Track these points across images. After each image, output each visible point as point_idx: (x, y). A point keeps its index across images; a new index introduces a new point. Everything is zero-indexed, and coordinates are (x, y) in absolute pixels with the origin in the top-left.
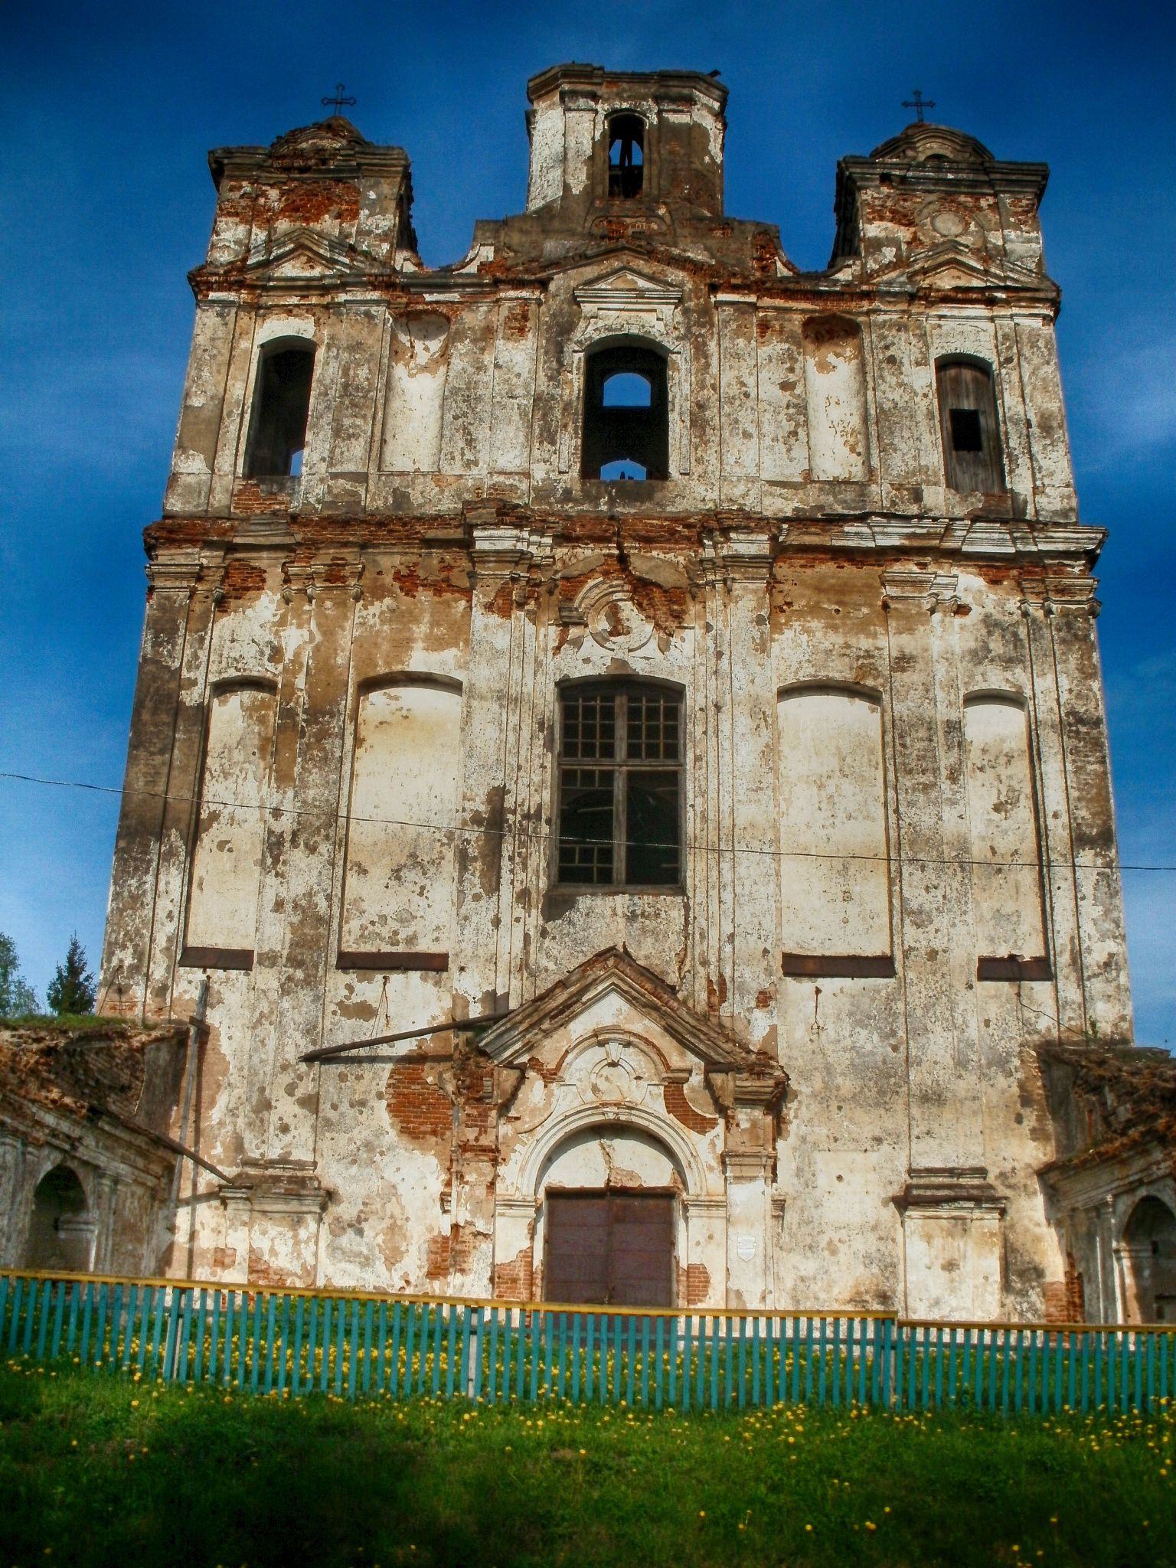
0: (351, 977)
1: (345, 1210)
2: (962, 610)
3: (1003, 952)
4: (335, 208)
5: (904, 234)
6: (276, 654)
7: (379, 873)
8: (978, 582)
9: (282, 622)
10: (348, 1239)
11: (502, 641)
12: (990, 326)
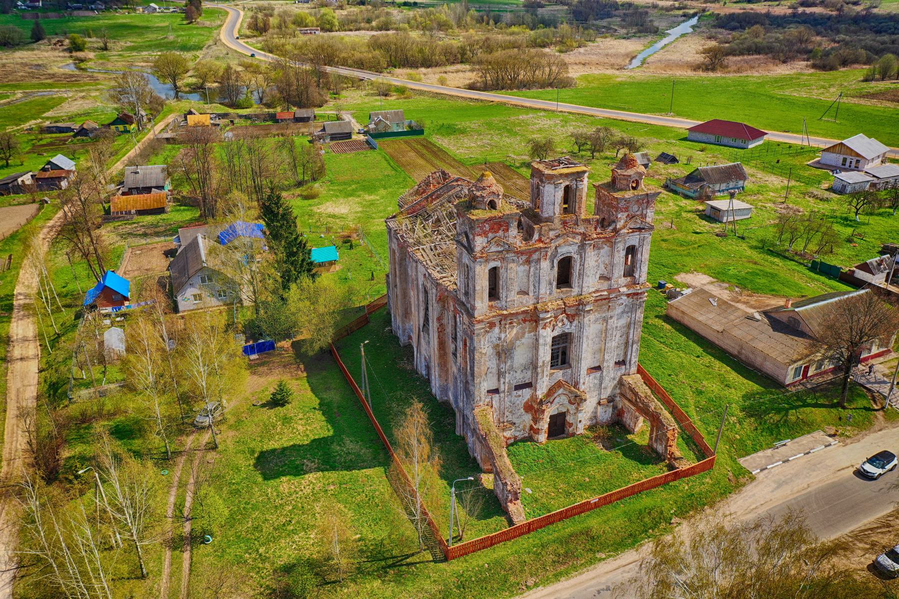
1: (517, 425)
3: (617, 361)
4: (502, 228)
5: (626, 214)
6: (500, 339)
7: (519, 372)
9: (501, 332)
10: (518, 429)
11: (545, 334)
12: (638, 236)
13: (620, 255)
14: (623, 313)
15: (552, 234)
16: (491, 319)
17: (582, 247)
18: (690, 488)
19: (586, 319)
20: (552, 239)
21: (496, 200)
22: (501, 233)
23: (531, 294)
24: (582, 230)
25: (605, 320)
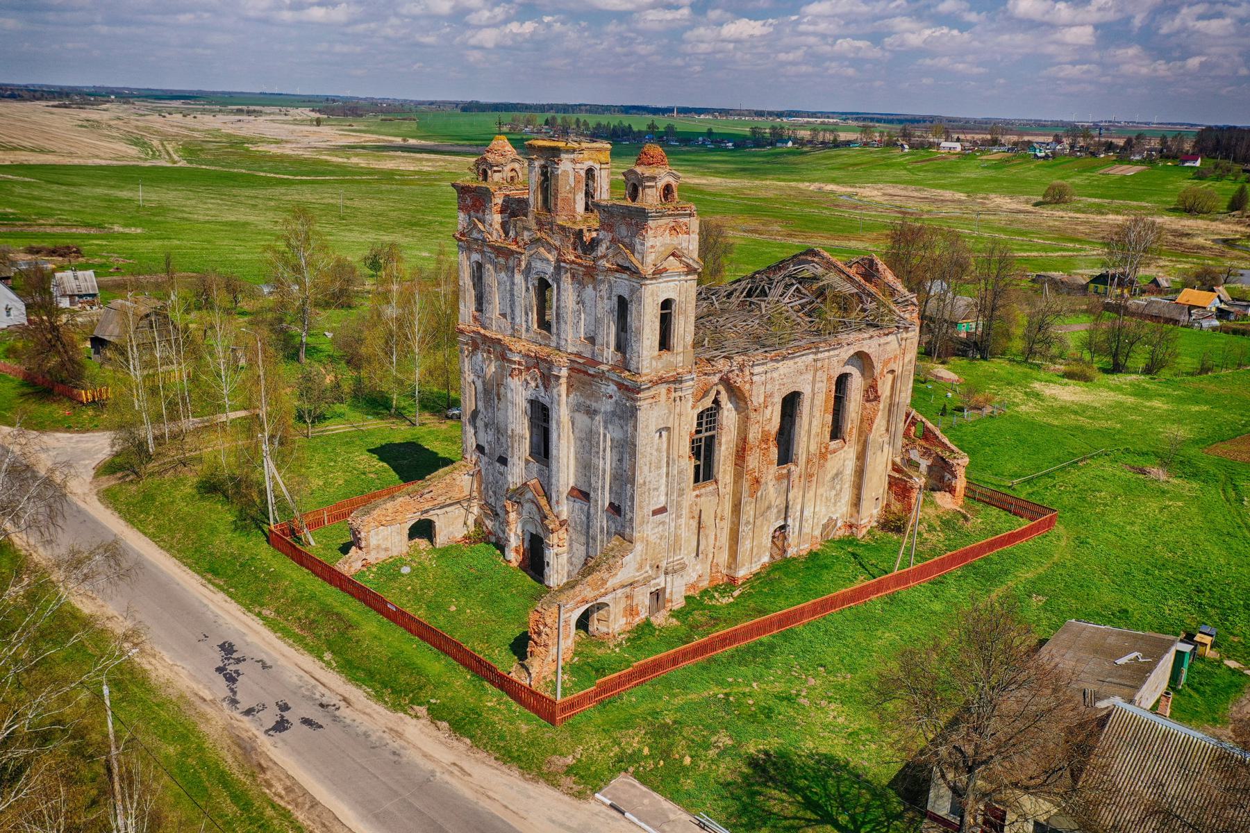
0: (498, 464)
2: (611, 397)
8: (615, 388)
11: (513, 386)
13: (606, 306)
14: (613, 413)
15: (526, 235)
16: (472, 334)
17: (558, 268)
18: (490, 709)
19: (555, 391)
20: (525, 244)
21: (489, 172)
22: (480, 215)
23: (509, 318)
24: (558, 243)
25: (591, 413)
